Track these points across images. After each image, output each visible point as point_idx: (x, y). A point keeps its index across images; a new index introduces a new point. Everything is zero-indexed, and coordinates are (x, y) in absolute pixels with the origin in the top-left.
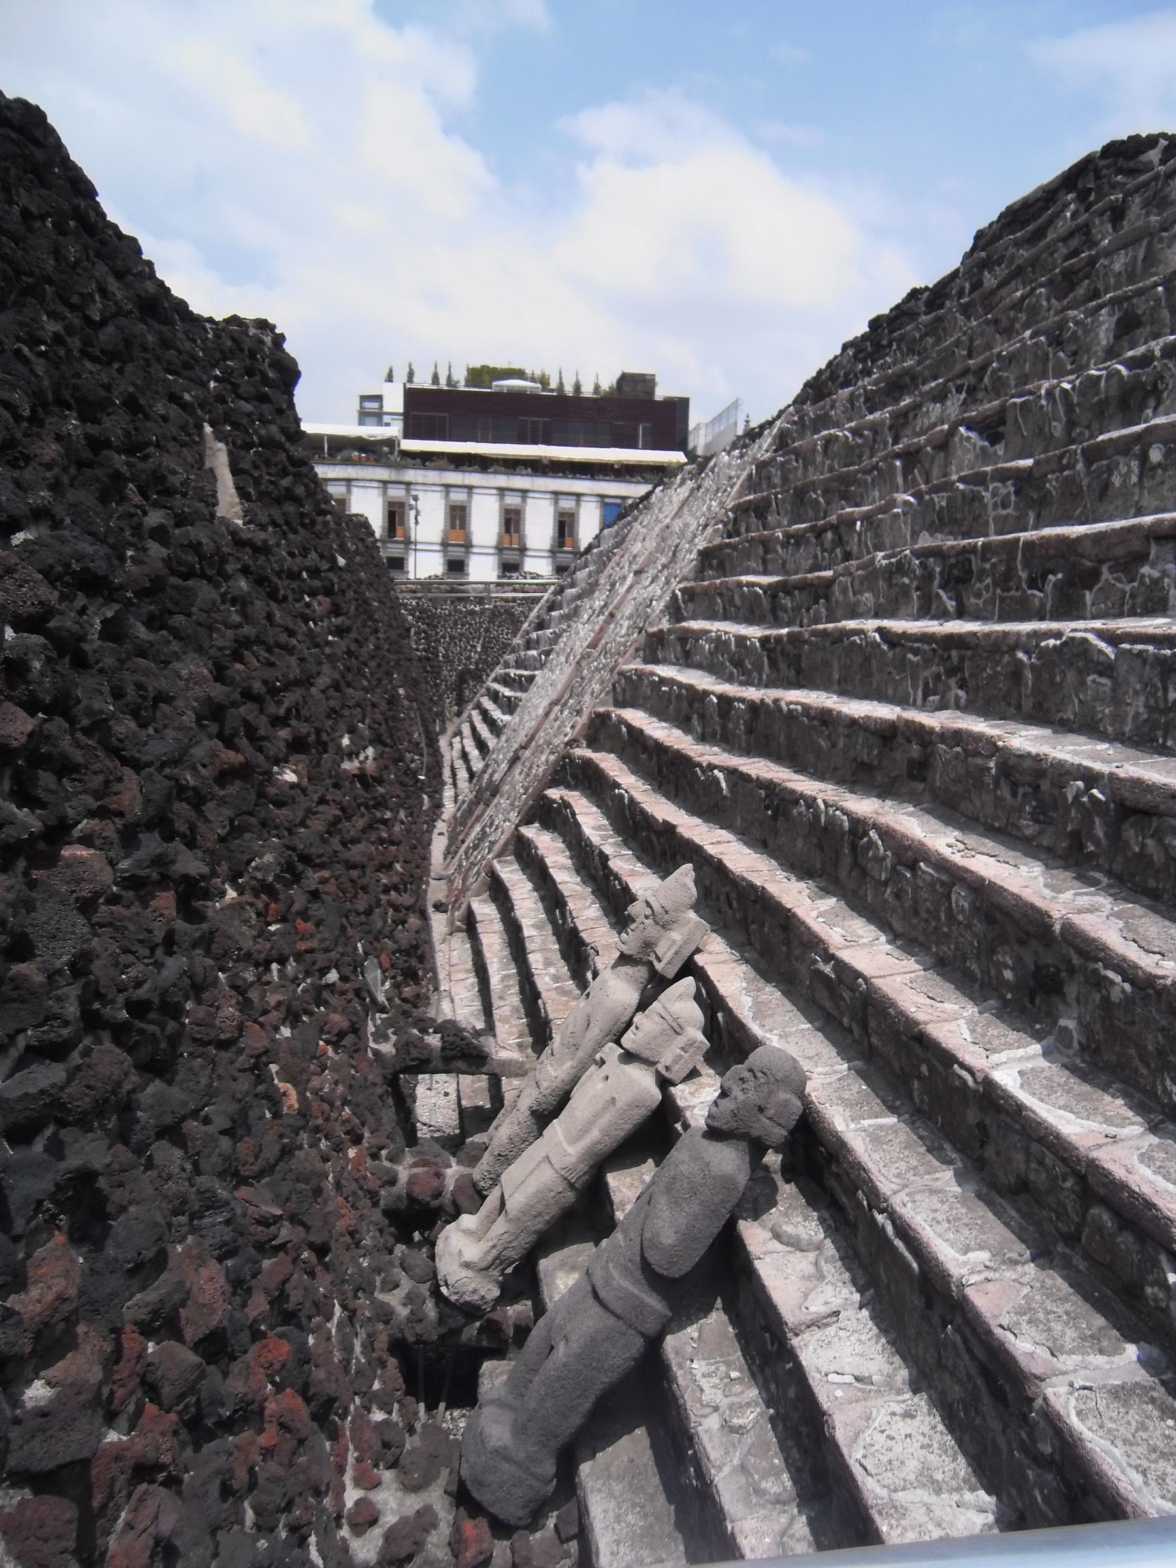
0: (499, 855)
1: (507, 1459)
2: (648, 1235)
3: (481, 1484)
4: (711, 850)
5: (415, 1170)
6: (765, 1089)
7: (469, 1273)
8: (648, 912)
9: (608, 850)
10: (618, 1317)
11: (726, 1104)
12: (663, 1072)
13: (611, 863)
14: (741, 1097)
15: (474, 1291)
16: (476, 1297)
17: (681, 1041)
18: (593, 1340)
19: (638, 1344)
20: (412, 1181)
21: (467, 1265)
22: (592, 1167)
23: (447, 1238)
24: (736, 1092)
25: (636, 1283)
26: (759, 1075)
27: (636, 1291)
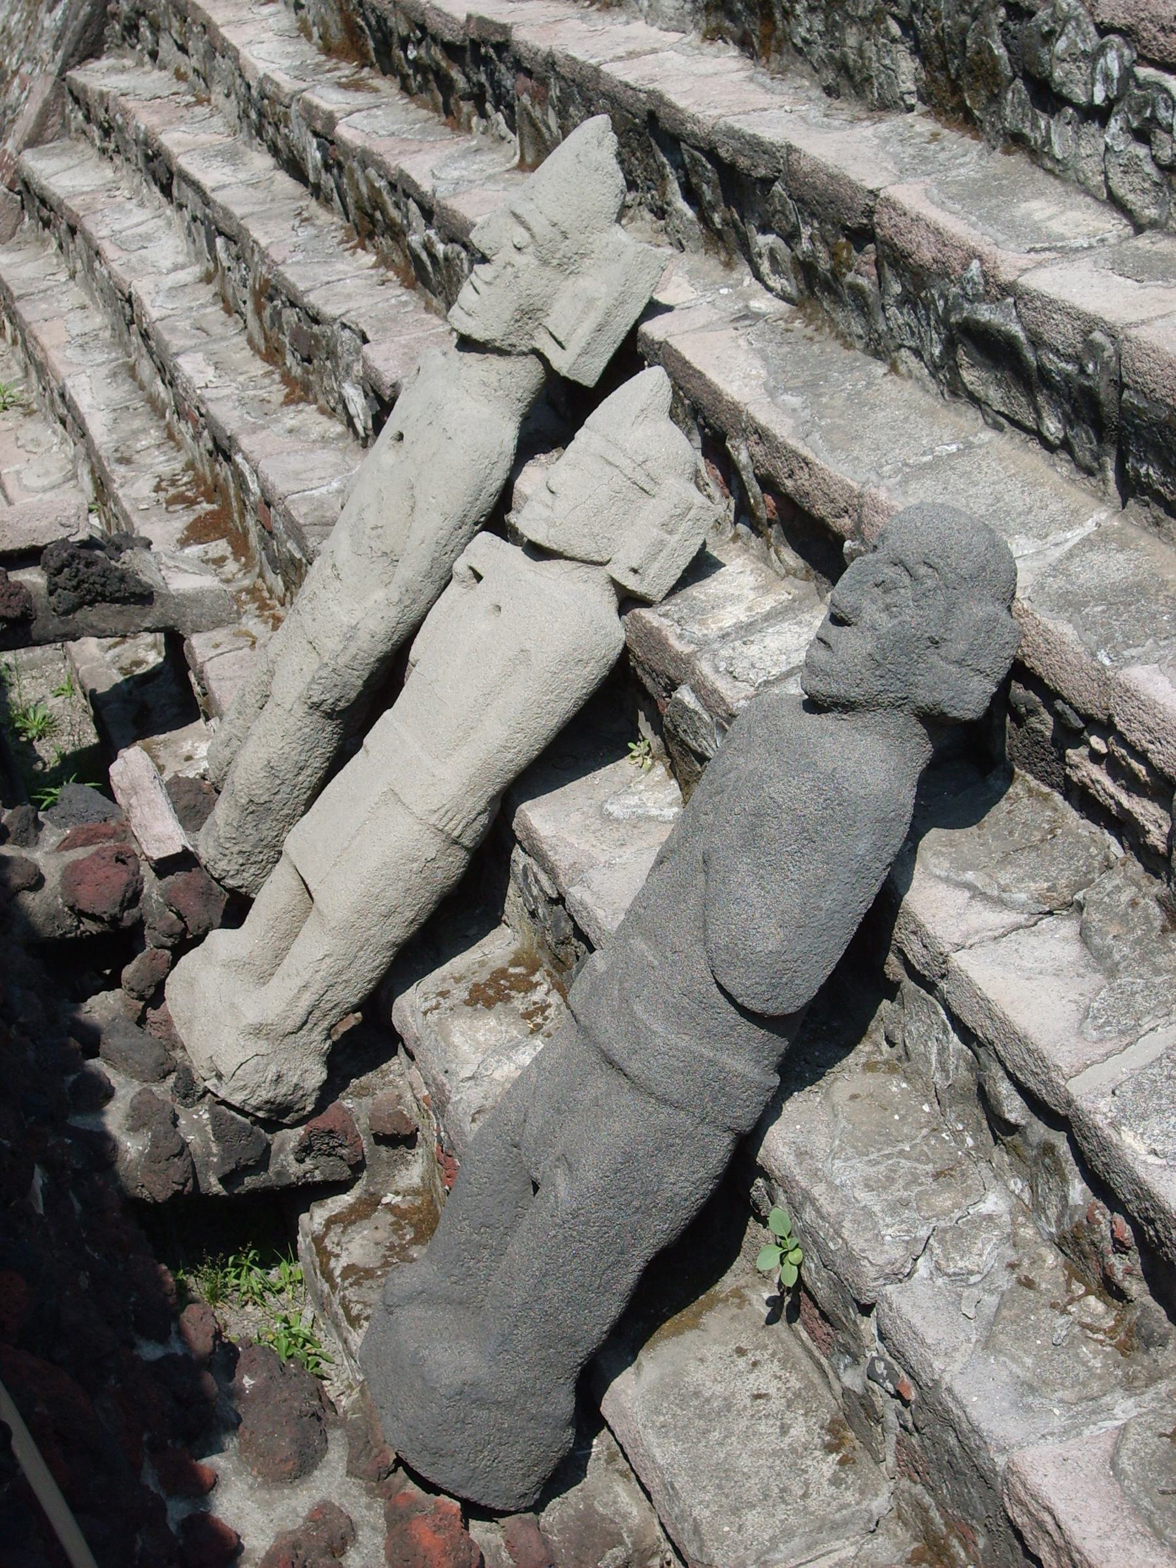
0: (34, 141)
1: (480, 1402)
2: (720, 937)
3: (438, 1453)
4: (623, 73)
5: (79, 854)
6: (940, 600)
7: (263, 1046)
8: (520, 236)
9: (328, 99)
10: (677, 1106)
11: (849, 641)
12: (631, 583)
13: (343, 131)
14: (885, 622)
15: (279, 1078)
16: (282, 1089)
17: (655, 510)
18: (629, 1158)
19: (721, 1147)
20: (72, 874)
21: (258, 1031)
22: (492, 801)
23: (191, 983)
24: (872, 612)
25: (709, 1035)
26: (923, 570)
27: (708, 1053)
